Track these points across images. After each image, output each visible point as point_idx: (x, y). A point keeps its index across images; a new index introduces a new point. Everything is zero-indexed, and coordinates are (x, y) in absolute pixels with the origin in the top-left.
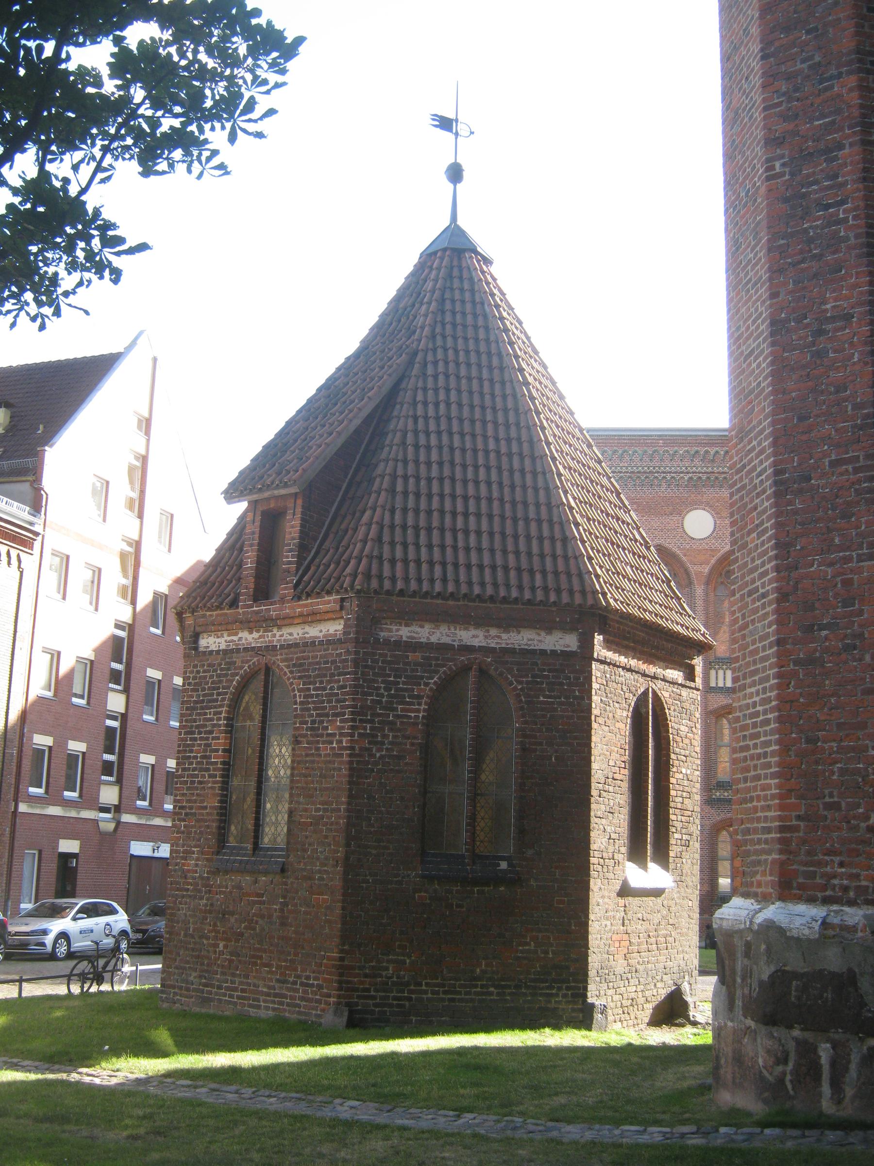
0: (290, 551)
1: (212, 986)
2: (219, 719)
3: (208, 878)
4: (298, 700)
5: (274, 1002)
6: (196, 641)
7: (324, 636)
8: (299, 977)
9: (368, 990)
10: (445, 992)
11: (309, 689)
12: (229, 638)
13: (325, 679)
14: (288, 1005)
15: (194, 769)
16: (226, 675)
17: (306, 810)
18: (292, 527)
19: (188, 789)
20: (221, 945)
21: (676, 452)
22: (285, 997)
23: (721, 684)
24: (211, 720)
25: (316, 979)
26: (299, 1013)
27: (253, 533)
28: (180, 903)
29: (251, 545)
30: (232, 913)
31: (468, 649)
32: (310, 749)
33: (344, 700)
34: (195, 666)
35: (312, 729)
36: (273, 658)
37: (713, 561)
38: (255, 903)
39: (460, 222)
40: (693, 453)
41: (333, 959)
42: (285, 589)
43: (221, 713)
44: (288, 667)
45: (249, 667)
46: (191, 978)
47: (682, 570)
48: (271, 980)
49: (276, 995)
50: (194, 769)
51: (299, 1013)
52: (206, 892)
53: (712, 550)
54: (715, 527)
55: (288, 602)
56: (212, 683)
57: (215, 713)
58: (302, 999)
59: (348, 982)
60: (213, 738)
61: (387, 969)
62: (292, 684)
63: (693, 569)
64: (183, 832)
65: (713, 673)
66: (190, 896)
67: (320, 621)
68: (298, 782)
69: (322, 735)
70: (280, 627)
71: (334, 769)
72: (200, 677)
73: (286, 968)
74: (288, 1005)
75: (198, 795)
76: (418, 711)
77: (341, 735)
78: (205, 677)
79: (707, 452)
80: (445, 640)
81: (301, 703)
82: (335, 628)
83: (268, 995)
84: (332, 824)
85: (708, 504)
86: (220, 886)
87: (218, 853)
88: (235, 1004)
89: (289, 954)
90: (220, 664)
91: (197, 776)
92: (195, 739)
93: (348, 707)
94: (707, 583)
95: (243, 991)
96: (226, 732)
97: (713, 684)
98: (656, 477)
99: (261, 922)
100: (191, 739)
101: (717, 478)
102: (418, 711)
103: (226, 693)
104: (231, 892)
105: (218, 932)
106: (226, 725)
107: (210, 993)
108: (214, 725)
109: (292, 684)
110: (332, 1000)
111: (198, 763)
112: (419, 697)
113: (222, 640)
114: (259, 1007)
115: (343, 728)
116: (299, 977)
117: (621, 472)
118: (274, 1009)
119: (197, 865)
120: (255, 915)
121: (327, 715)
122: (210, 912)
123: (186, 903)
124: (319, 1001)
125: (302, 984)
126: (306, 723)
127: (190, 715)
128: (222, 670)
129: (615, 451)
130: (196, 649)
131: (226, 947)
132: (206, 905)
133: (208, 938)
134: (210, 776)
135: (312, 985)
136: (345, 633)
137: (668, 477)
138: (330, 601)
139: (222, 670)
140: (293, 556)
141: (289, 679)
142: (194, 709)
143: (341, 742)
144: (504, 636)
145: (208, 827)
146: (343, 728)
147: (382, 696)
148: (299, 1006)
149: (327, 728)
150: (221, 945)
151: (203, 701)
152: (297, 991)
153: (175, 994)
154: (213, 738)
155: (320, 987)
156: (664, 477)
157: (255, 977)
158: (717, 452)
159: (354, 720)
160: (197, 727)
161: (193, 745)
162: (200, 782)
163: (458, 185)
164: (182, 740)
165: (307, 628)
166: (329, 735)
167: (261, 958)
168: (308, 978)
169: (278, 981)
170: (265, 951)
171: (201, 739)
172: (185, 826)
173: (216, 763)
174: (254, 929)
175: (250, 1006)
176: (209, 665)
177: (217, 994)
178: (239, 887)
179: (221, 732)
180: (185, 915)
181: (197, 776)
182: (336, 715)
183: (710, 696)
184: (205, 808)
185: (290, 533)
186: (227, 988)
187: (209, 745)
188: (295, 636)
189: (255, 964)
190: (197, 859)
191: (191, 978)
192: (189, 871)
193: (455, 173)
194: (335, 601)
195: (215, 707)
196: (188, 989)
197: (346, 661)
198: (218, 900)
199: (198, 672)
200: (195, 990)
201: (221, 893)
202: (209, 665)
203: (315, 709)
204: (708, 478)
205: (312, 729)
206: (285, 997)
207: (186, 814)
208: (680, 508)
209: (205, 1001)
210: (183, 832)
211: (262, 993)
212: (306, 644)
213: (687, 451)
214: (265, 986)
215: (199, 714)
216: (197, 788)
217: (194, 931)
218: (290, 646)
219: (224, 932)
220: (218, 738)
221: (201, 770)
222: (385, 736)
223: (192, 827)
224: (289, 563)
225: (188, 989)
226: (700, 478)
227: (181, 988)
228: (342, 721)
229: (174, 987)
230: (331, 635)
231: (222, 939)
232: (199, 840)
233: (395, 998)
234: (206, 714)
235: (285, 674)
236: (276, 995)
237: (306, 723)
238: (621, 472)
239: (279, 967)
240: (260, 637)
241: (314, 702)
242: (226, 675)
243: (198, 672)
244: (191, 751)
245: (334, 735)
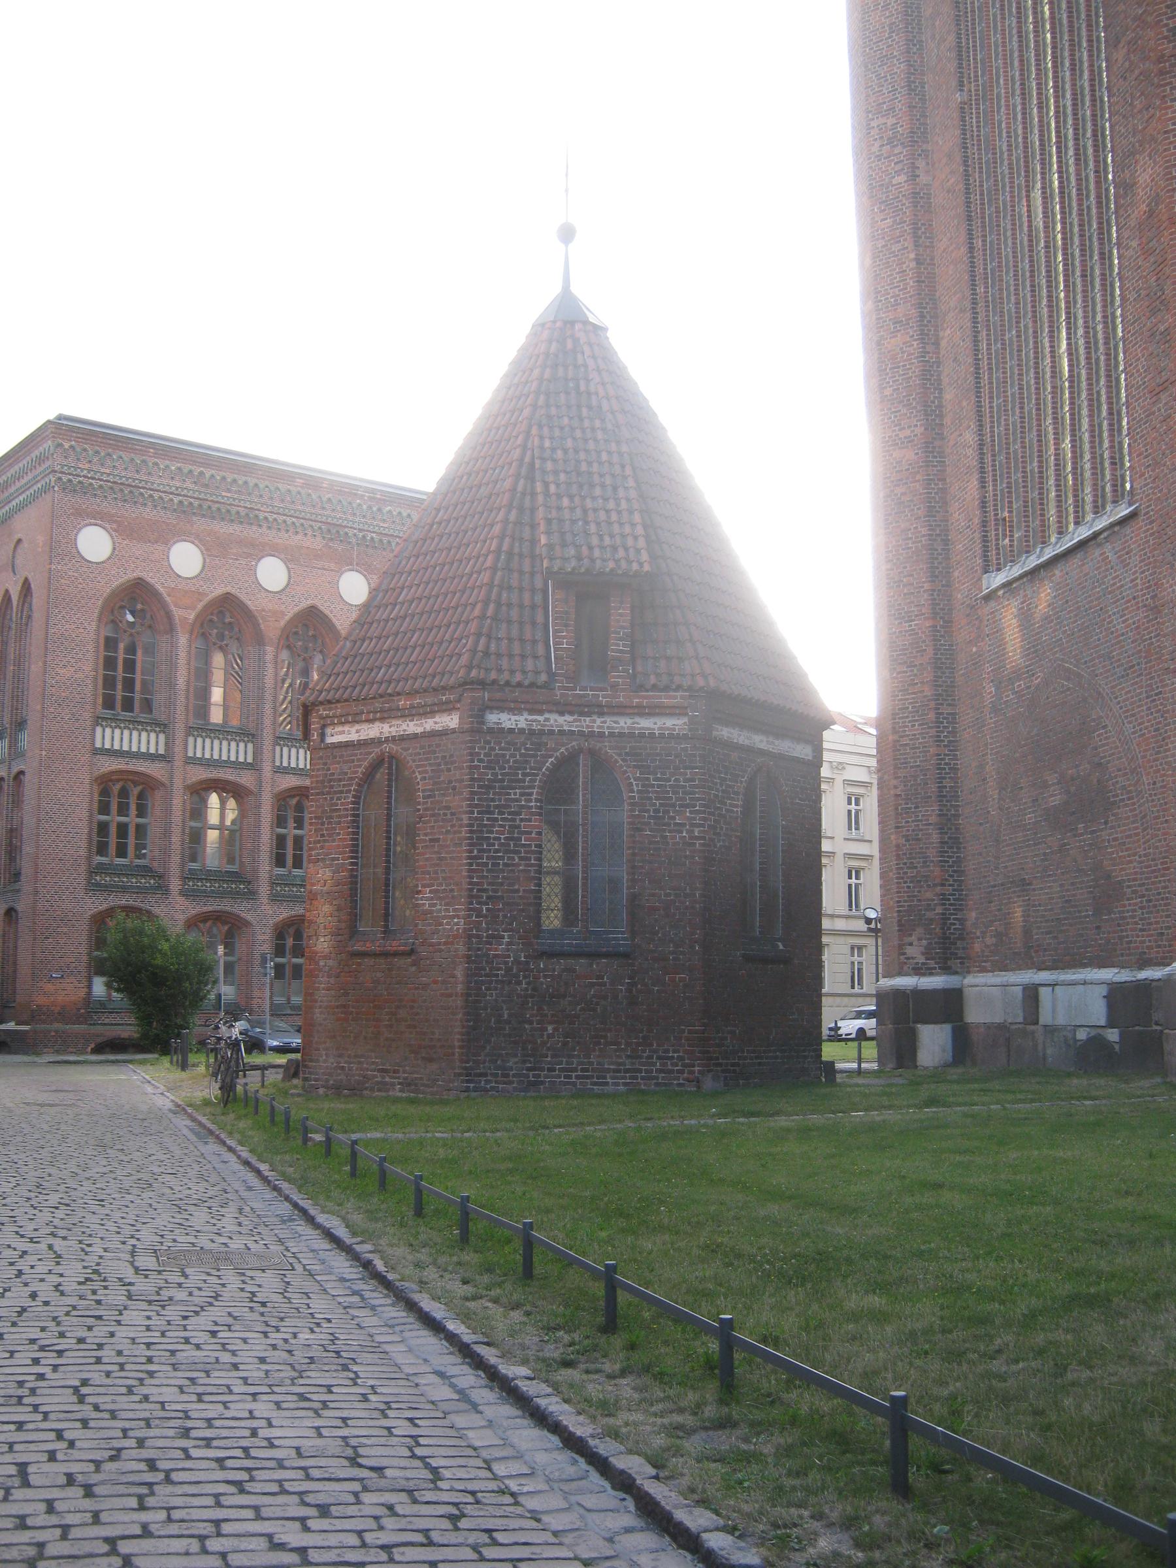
0: (621, 639)
1: (542, 1069)
2: (531, 801)
3: (527, 963)
4: (635, 788)
5: (624, 1078)
6: (482, 716)
7: (660, 729)
8: (655, 1051)
9: (717, 1058)
10: (756, 1058)
11: (648, 779)
12: (530, 717)
13: (668, 771)
14: (643, 1078)
15: (497, 851)
16: (535, 756)
17: (653, 895)
18: (621, 615)
19: (488, 871)
20: (550, 1029)
21: (167, 466)
22: (640, 1071)
23: (143, 750)
24: (517, 800)
25: (674, 1052)
26: (657, 1084)
27: (567, 613)
28: (488, 989)
29: (566, 625)
30: (564, 996)
31: (762, 752)
32: (655, 837)
33: (695, 793)
34: (489, 743)
35: (654, 818)
36: (599, 745)
37: (200, 606)
38: (592, 985)
39: (575, 289)
40: (186, 471)
41: (696, 1032)
42: (619, 677)
43: (531, 794)
44: (620, 755)
45: (567, 750)
46: (510, 1064)
47: (162, 613)
48: (619, 1057)
49: (627, 1071)
50: (497, 851)
51: (657, 1084)
52: (525, 977)
53: (200, 594)
54: (204, 566)
55: (623, 690)
56: (515, 762)
57: (522, 794)
58: (660, 1071)
59: (708, 1052)
60: (522, 820)
61: (726, 1038)
62: (626, 772)
63: (177, 613)
64: (486, 916)
65: (99, 730)
66: (503, 982)
67: (666, 714)
68: (642, 867)
69: (669, 825)
70: (601, 714)
71: (686, 857)
72: (496, 755)
73: (638, 1044)
74: (643, 1078)
75: (503, 877)
76: (736, 806)
77: (692, 825)
78: (504, 756)
79: (201, 473)
80: (747, 742)
81: (639, 792)
82: (674, 723)
83: (619, 1071)
84: (687, 908)
85: (197, 536)
86: (544, 970)
87: (537, 937)
88: (574, 1084)
89: (642, 1031)
90: (524, 744)
91: (502, 858)
92: (496, 820)
93: (699, 799)
94: (191, 633)
95: (583, 1070)
96: (540, 814)
97: (190, 754)
98: (142, 494)
99: (603, 1002)
100: (488, 819)
101: (210, 507)
102: (736, 806)
103: (537, 775)
104: (560, 976)
105: (546, 1015)
106: (541, 808)
107: (539, 1076)
108: (522, 807)
109: (626, 772)
110: (697, 1068)
111: (501, 845)
112: (737, 793)
113: (522, 718)
114: (607, 1084)
115: (695, 819)
116: (655, 1051)
117: (101, 480)
118: (625, 1084)
119: (508, 950)
120: (594, 996)
121: (674, 806)
122: (532, 996)
123: (496, 989)
124: (681, 1072)
125: (659, 1058)
126: (648, 811)
127: (485, 793)
128: (526, 749)
129: (97, 452)
130: (483, 723)
131: (555, 1029)
132: (526, 989)
133: (531, 1023)
134: (521, 859)
135: (673, 1057)
136: (690, 730)
137: (156, 495)
138: (677, 698)
139: (526, 749)
140: (624, 646)
141: (621, 766)
142: (489, 787)
143: (693, 831)
144: (777, 742)
145: (523, 910)
146: (695, 819)
147: (717, 790)
148: (657, 1078)
149: (674, 818)
150: (550, 1029)
151: (502, 781)
152: (654, 1064)
153: (487, 1082)
154: (522, 820)
155: (681, 1058)
156: (151, 496)
157: (599, 1056)
158: (213, 476)
159: (704, 812)
160: (496, 807)
161: (493, 826)
162: (505, 865)
163: (570, 246)
164: (476, 819)
165: (637, 719)
166: (676, 824)
167: (605, 1037)
168: (667, 1051)
169: (628, 1057)
170: (610, 1030)
171: (503, 819)
172: (488, 910)
173: (530, 845)
174: (594, 1010)
175: (595, 1084)
176: (508, 743)
177: (546, 1077)
178: (571, 970)
179: (533, 814)
180: (496, 1000)
181: (502, 858)
182: (687, 806)
183: (189, 767)
184: (517, 891)
185: (618, 621)
186: (561, 1070)
187: (519, 827)
188: (622, 724)
189: (599, 1044)
190: (509, 944)
191: (510, 1064)
192: (496, 956)
193: (567, 234)
194: (682, 697)
195: (523, 788)
196: (507, 1076)
197: (695, 756)
198: (542, 983)
199: (493, 749)
200: (514, 1076)
201: (545, 977)
202: (508, 743)
203: (657, 798)
204: (200, 506)
205: (654, 818)
206: (640, 1071)
207: (488, 898)
208: (166, 537)
209: (535, 1084)
210: (486, 916)
211: (609, 1070)
212: (642, 735)
213: (179, 469)
214: (612, 1064)
215: (500, 794)
216: (503, 871)
217: (510, 1015)
218: (621, 735)
219: (553, 1016)
220: (530, 820)
221: (506, 852)
222: (721, 828)
223: (499, 910)
224: (621, 651)
225: (504, 1076)
226: (191, 503)
227: (496, 1075)
228: (691, 812)
229: (485, 1075)
230: (668, 729)
231: (550, 1023)
232: (511, 924)
233: (733, 1065)
234: (509, 794)
235: (616, 761)
236: (627, 1071)
237: (648, 811)
238: (101, 480)
239: (627, 1044)
240: (575, 720)
241: (657, 792)
242: (535, 756)
243: (493, 749)
244: (492, 832)
245: (683, 825)
